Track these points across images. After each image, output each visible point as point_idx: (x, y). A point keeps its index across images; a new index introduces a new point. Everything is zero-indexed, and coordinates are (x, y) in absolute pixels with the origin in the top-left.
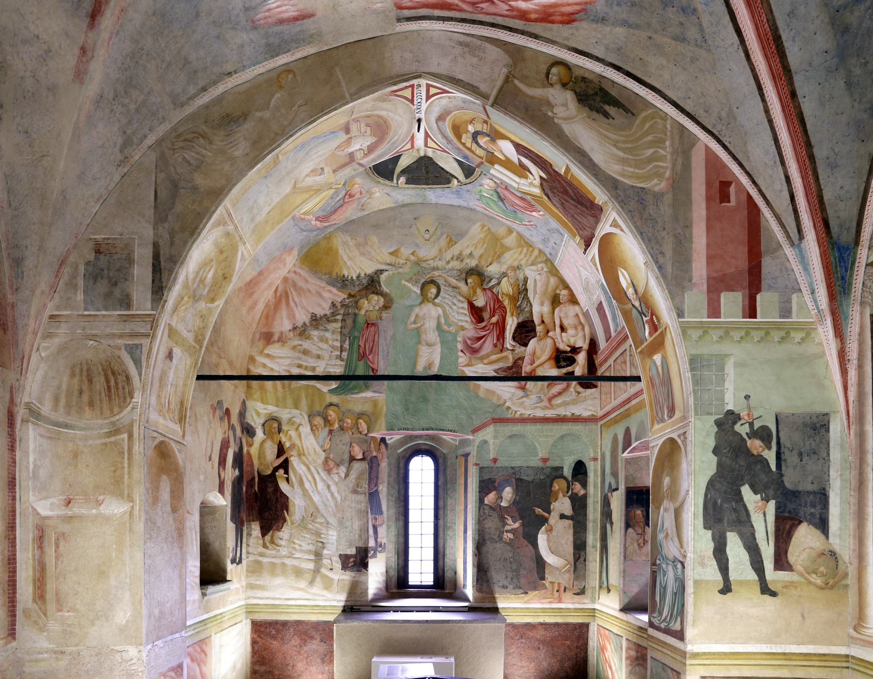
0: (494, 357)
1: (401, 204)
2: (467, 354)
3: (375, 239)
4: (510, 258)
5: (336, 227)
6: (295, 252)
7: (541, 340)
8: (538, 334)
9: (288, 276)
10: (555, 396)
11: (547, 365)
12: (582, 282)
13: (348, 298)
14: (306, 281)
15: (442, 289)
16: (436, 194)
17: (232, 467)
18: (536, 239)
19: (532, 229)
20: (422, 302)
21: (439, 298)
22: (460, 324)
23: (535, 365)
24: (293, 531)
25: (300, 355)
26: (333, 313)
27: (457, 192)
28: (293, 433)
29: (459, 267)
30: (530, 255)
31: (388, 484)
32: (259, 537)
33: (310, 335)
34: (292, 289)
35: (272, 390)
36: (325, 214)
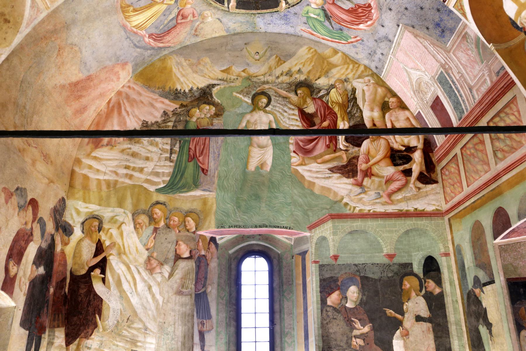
0: (327, 157)
1: (232, 32)
2: (300, 155)
3: (207, 60)
4: (337, 74)
5: (171, 50)
6: (129, 68)
10: (394, 192)
11: (382, 164)
12: (412, 85)
13: (180, 108)
14: (140, 94)
15: (273, 99)
17: (34, 263)
18: (362, 57)
21: (270, 106)
23: (370, 163)
24: (104, 339)
25: (128, 157)
26: (164, 120)
27: (285, 17)
28: (114, 232)
29: (288, 81)
30: (357, 70)
31: (218, 285)
32: (62, 346)
34: (125, 101)
35: (96, 190)
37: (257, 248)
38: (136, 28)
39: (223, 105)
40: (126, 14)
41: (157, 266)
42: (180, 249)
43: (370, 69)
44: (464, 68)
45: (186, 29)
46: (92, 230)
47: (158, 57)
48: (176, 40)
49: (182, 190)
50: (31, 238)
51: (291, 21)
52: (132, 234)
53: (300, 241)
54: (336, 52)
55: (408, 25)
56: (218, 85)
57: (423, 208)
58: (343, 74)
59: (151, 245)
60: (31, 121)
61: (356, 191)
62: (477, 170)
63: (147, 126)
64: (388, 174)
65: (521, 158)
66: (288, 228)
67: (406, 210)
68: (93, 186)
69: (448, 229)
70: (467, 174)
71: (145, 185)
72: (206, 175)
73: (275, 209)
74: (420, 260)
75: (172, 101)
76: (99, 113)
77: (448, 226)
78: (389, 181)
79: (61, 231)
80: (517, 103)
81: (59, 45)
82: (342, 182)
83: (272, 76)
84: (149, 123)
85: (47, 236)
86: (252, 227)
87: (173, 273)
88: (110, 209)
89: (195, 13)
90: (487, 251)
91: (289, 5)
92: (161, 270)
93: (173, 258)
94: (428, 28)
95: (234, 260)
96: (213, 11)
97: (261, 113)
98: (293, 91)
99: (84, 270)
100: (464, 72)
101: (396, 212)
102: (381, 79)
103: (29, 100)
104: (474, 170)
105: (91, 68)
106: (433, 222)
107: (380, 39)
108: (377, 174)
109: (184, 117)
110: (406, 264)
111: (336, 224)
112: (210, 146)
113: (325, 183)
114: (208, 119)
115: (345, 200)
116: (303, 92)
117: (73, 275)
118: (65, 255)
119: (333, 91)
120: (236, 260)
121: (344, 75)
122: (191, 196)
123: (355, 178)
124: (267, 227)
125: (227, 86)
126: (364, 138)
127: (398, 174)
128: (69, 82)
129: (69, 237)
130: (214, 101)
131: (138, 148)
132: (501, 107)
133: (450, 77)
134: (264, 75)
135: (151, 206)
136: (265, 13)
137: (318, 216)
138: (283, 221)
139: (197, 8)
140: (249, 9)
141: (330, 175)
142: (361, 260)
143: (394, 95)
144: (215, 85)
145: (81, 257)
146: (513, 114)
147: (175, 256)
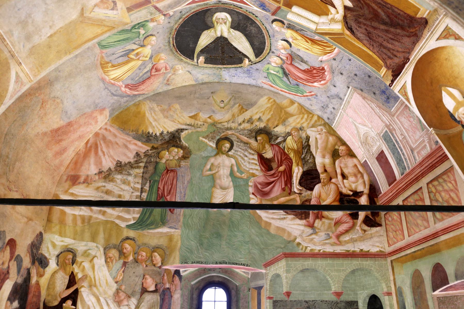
1: (201, 82)
2: (258, 196)
3: (177, 106)
4: (293, 122)
5: (146, 96)
7: (325, 185)
8: (322, 181)
9: (99, 131)
13: (151, 150)
14: (115, 136)
15: (235, 144)
16: (230, 74)
17: (9, 299)
19: (313, 99)
20: (217, 154)
21: (232, 151)
22: (251, 171)
26: (136, 161)
29: (249, 128)
30: (311, 120)
33: (114, 178)
34: (102, 142)
36: (133, 82)
37: (217, 279)
38: (114, 80)
39: (190, 148)
40: (105, 69)
41: (125, 298)
42: (146, 283)
43: (322, 119)
44: (406, 131)
45: (159, 80)
46: (66, 263)
47: (133, 102)
48: (149, 89)
49: (151, 227)
50: (7, 276)
51: (253, 75)
52: (103, 267)
53: (256, 276)
54: (292, 102)
55: (357, 88)
56: (186, 129)
57: (368, 250)
58: (298, 123)
59: (120, 278)
60: (13, 168)
61: (308, 232)
62: (418, 224)
63: (121, 166)
64: (337, 216)
65: (458, 224)
66: (246, 265)
67: (353, 251)
68: (69, 220)
69: (390, 270)
70: (408, 225)
71: (117, 221)
72: (173, 213)
73: (234, 246)
74: (365, 298)
75: (145, 143)
76: (77, 152)
77: (390, 268)
78: (338, 223)
79: (37, 263)
80: (454, 173)
81: (42, 99)
82: (295, 223)
83: (235, 123)
84: (122, 163)
85: (24, 272)
86: (213, 263)
87: (139, 306)
88: (84, 243)
89: (167, 67)
90: (426, 300)
91: (252, 62)
92: (128, 303)
93: (140, 291)
94: (374, 93)
95: (196, 290)
96: (184, 65)
97: (224, 157)
98: (253, 138)
99: (56, 301)
100: (406, 134)
101: (343, 252)
102: (332, 129)
103: (12, 150)
104: (414, 223)
105: (71, 115)
106: (377, 262)
107: (332, 96)
108: (327, 216)
109: (155, 159)
110: (352, 301)
111: (290, 263)
112: (177, 186)
113: (280, 223)
114: (176, 161)
115: (298, 240)
116: (263, 138)
117: (46, 306)
118: (40, 287)
119: (290, 138)
120: (197, 290)
121: (299, 124)
122: (158, 232)
123: (307, 220)
124: (226, 263)
125: (194, 131)
126: (316, 183)
127: (346, 217)
128: (50, 129)
129: (44, 269)
130: (182, 145)
131: (111, 186)
132: (439, 173)
133: (394, 137)
134: (228, 122)
135: (121, 242)
136: (230, 68)
137: (273, 255)
138: (241, 258)
139: (169, 63)
140: (216, 64)
141: (285, 216)
142: (311, 297)
143: (344, 144)
144: (184, 129)
145: (54, 289)
146: (451, 182)
147: (142, 289)
